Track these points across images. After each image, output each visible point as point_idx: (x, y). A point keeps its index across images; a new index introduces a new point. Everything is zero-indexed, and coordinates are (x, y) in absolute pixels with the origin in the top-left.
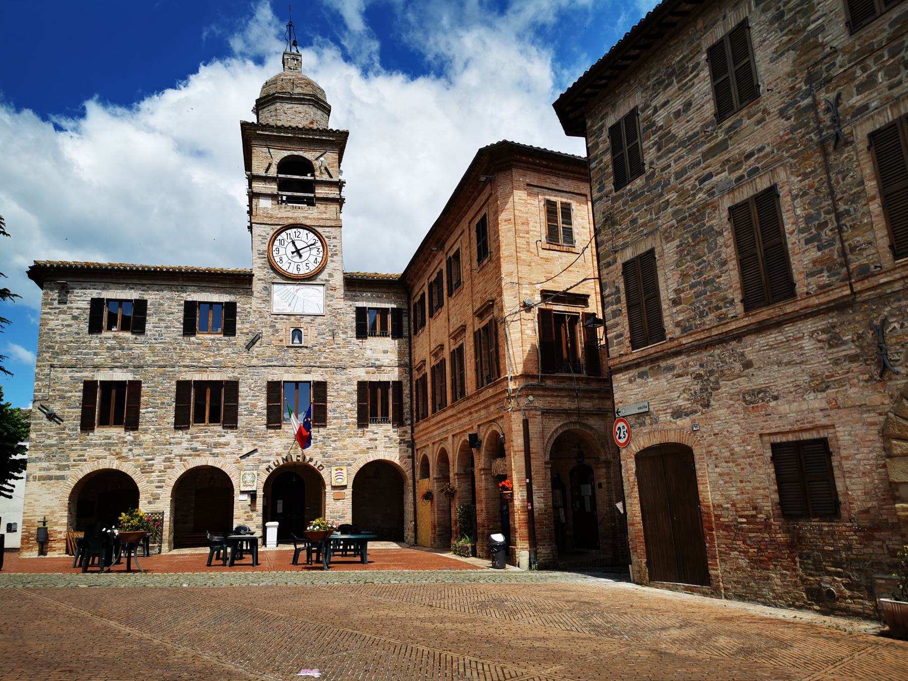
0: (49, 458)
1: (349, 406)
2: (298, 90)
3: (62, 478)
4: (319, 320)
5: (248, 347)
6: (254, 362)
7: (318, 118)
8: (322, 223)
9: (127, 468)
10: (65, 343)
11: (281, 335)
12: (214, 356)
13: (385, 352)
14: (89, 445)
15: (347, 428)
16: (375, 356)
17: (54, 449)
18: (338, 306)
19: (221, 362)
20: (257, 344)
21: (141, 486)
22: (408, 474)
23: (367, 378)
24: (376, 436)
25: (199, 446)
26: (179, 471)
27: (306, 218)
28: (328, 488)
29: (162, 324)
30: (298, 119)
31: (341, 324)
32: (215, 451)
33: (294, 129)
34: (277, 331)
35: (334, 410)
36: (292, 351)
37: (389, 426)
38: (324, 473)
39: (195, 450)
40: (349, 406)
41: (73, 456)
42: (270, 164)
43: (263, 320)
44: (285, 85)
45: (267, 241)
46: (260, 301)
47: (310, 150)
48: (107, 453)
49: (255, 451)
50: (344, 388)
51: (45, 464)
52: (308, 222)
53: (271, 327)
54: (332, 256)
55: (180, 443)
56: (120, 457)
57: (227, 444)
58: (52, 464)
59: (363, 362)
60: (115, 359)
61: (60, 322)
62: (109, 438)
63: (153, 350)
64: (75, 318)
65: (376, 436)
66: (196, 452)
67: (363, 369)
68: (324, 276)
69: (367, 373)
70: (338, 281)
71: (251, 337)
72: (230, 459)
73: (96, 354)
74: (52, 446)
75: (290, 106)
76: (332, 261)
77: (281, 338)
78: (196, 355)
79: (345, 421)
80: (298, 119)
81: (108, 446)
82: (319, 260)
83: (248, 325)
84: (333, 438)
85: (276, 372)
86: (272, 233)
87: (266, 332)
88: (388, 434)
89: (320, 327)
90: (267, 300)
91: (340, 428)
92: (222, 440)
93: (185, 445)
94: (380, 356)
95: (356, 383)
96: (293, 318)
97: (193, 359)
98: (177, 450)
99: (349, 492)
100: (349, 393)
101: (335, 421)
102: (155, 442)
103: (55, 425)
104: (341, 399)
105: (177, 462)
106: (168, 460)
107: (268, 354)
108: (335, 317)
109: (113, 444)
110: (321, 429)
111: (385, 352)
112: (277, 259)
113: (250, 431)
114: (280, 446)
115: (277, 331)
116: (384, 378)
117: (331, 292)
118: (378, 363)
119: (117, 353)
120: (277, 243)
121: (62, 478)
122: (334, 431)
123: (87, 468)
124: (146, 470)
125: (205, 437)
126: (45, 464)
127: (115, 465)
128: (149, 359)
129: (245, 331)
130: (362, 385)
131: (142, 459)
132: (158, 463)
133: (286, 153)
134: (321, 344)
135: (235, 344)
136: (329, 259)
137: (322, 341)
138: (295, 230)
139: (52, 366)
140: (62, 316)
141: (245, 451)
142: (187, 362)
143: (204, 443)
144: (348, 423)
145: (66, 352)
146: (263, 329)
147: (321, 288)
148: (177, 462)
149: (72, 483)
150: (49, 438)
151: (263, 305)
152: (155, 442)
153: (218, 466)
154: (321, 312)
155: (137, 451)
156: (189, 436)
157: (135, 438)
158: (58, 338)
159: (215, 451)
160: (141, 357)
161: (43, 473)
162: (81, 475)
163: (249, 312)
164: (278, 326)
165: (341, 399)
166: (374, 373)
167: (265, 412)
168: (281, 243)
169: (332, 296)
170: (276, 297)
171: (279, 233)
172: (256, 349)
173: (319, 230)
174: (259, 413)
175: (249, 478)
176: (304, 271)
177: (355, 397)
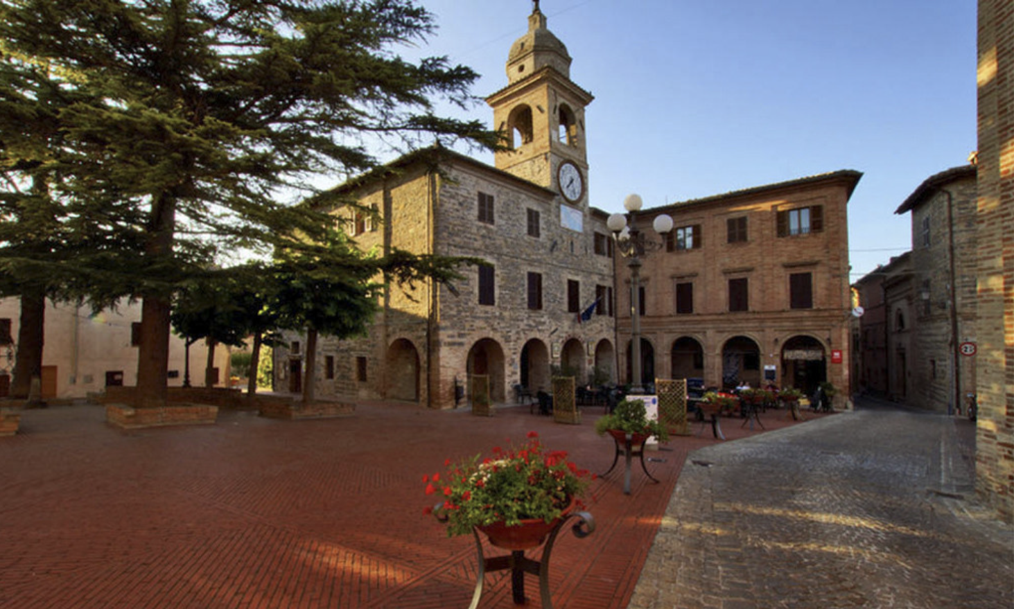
0: (453, 326)
3: (461, 344)
4: (581, 237)
6: (555, 263)
9: (497, 337)
10: (455, 225)
14: (475, 317)
17: (455, 319)
21: (506, 351)
22: (614, 346)
25: (533, 324)
26: (523, 343)
28: (587, 357)
29: (510, 222)
32: (540, 328)
34: (563, 241)
38: (585, 345)
39: (530, 326)
41: (467, 326)
47: (574, 104)
48: (485, 325)
49: (556, 330)
51: (450, 332)
55: (522, 320)
56: (494, 330)
57: (544, 323)
58: (455, 332)
59: (596, 271)
60: (487, 247)
61: (450, 205)
62: (486, 312)
63: (506, 241)
64: (461, 204)
66: (531, 328)
68: (581, 204)
70: (586, 210)
72: (547, 334)
73: (475, 240)
74: (454, 316)
78: (528, 251)
81: (486, 319)
90: (558, 216)
92: (543, 320)
93: (525, 322)
98: (522, 325)
99: (593, 358)
102: (511, 319)
103: (456, 299)
105: (522, 335)
106: (518, 333)
109: (488, 318)
114: (567, 327)
119: (488, 241)
121: (461, 344)
123: (476, 337)
124: (507, 340)
126: (450, 332)
127: (491, 335)
128: (505, 250)
131: (505, 331)
132: (513, 335)
133: (561, 100)
139: (449, 245)
140: (452, 201)
141: (553, 329)
142: (524, 256)
143: (534, 321)
145: (457, 235)
147: (580, 213)
148: (522, 335)
149: (467, 348)
150: (451, 309)
152: (511, 319)
153: (541, 338)
155: (502, 325)
157: (501, 314)
158: (451, 220)
159: (540, 328)
160: (500, 247)
161: (450, 340)
162: (473, 342)
164: (565, 238)
170: (562, 215)
172: (556, 253)
175: (556, 349)
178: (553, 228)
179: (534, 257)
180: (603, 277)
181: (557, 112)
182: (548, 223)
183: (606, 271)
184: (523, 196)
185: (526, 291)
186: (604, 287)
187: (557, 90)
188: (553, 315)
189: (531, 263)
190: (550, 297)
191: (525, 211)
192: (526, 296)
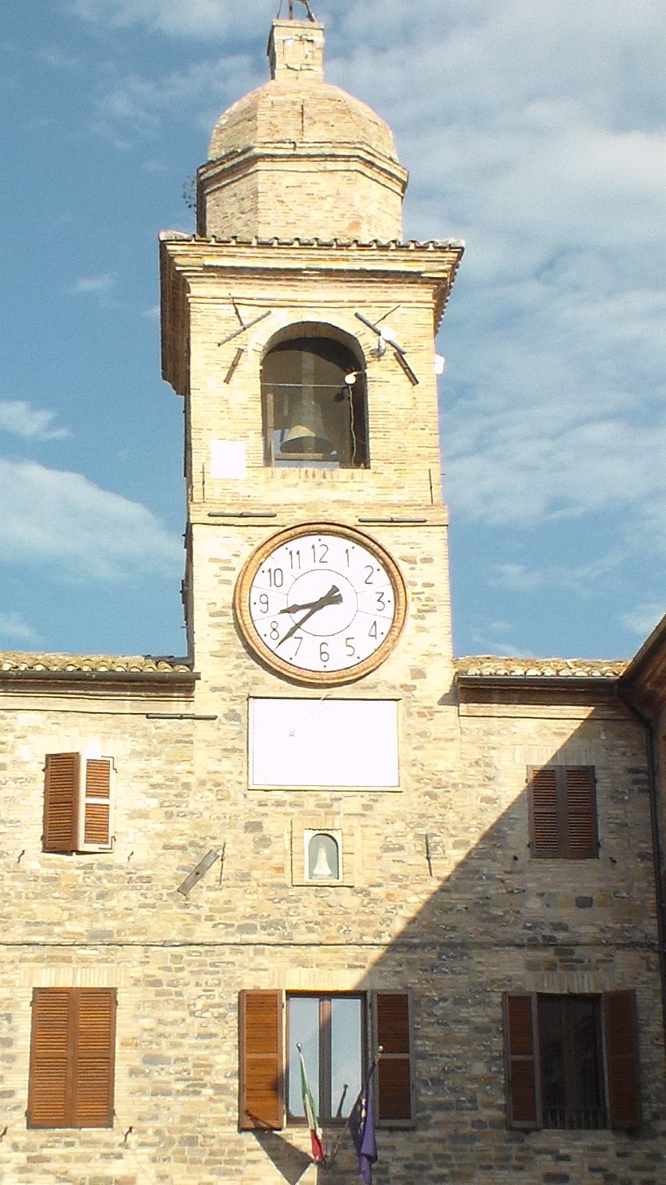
1: (479, 1068)
2: (315, 133)
4: (387, 806)
5: (184, 889)
6: (204, 932)
7: (372, 209)
8: (386, 514)
11: (277, 852)
12: (93, 916)
13: (584, 903)
15: (472, 1138)
16: (552, 915)
18: (442, 765)
19: (110, 934)
20: (211, 876)
23: (532, 984)
24: (564, 1167)
27: (345, 504)
30: (317, 216)
31: (451, 816)
33: (306, 245)
34: (265, 842)
35: (437, 1082)
36: (310, 898)
37: (604, 1138)
40: (479, 1068)
42: (240, 351)
43: (227, 808)
44: (279, 121)
45: (233, 576)
46: (217, 753)
50: (464, 1013)
52: (349, 518)
53: (253, 827)
54: (421, 614)
65: (564, 1167)
67: (516, 953)
69: (531, 966)
71: (192, 858)
75: (291, 179)
76: (422, 629)
77: (277, 860)
78: (41, 911)
79: (468, 1116)
80: (317, 216)
82: (384, 626)
83: (184, 825)
84: (437, 1171)
85: (261, 960)
86: (247, 551)
87: (238, 845)
88: (603, 1161)
89: (389, 830)
91: (456, 1138)
94: (568, 914)
95: (497, 999)
96: (310, 803)
97: (33, 924)
100: (482, 1030)
101: (439, 1116)
104: (456, 1049)
107: (243, 905)
108: (433, 796)
110: (400, 1138)
111: (584, 903)
112: (264, 627)
113: (192, 1141)
115: (265, 842)
116: (585, 983)
117: (420, 724)
118: (561, 936)
120: (262, 579)
122: (437, 1148)
125: (66, 1159)
129: (176, 841)
130: (516, 1004)
133: (282, 319)
134: (394, 878)
135: (149, 880)
136: (410, 622)
137: (396, 869)
138: (313, 539)
144: (479, 1124)
146: (228, 836)
151: (226, 765)
154: (391, 781)
156: (21, 1157)
163: (186, 785)
164: (270, 827)
165: (456, 1049)
166: (552, 967)
167: (235, 1083)
168: (273, 581)
169: (422, 734)
171: (268, 548)
172: (204, 895)
173: (383, 536)
174: (220, 1089)
176: (339, 660)
177: (498, 1043)
178: (194, 803)
179: (78, 927)
180: (566, 955)
181: (252, 366)
182: (172, 795)
183: (585, 926)
184: (24, 719)
185: (24, 1063)
186: (593, 999)
187: (240, 289)
188: (186, 1144)
189: (59, 950)
190: (165, 1075)
191: (36, 770)
192: (19, 1081)
